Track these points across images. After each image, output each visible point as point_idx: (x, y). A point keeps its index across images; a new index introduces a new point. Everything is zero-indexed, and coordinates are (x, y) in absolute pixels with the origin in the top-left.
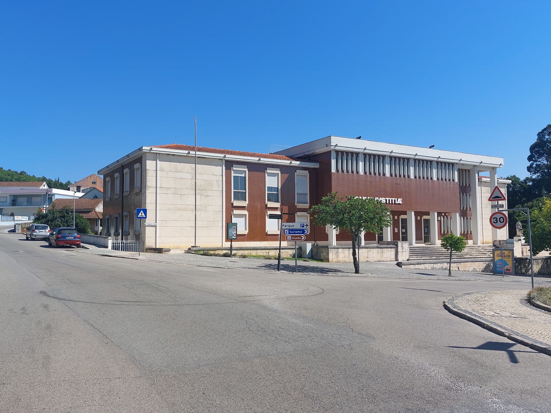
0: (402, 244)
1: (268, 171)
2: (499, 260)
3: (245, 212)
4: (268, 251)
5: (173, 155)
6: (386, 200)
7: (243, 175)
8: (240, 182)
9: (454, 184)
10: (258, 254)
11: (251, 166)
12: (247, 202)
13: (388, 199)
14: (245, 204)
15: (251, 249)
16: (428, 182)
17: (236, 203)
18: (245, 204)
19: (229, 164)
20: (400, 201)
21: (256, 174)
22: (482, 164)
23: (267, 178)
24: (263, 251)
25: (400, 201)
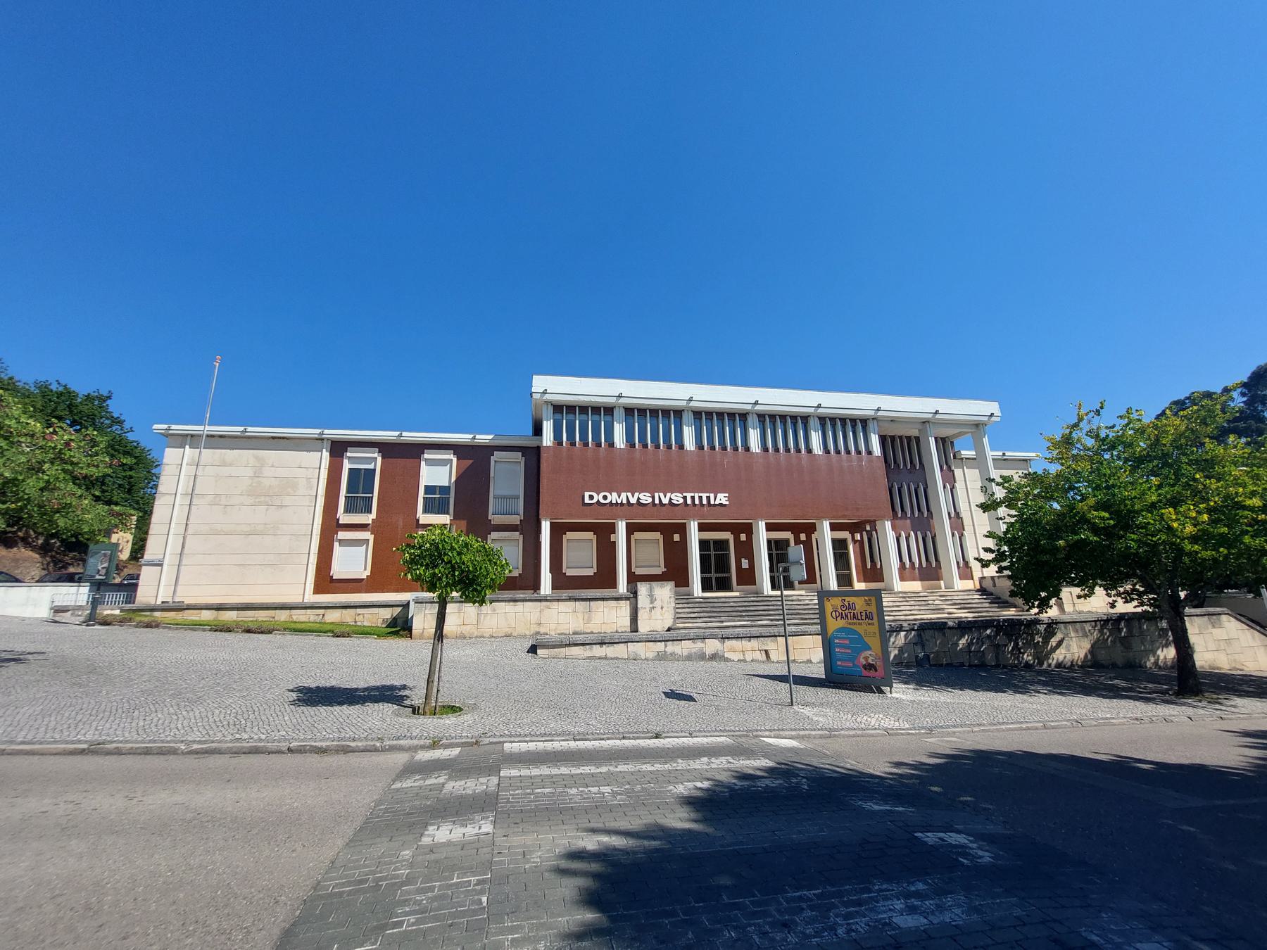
0: (651, 589)
1: (426, 456)
2: (840, 630)
3: (367, 535)
4: (322, 611)
5: (221, 436)
6: (685, 498)
7: (371, 467)
8: (361, 480)
9: (870, 461)
10: (295, 618)
11: (386, 449)
12: (373, 515)
13: (689, 495)
14: (368, 519)
15: (276, 608)
16: (800, 459)
17: (344, 518)
18: (368, 519)
19: (338, 449)
20: (722, 498)
21: (400, 462)
22: (880, 413)
23: (424, 467)
24: (309, 611)
25: (722, 498)
